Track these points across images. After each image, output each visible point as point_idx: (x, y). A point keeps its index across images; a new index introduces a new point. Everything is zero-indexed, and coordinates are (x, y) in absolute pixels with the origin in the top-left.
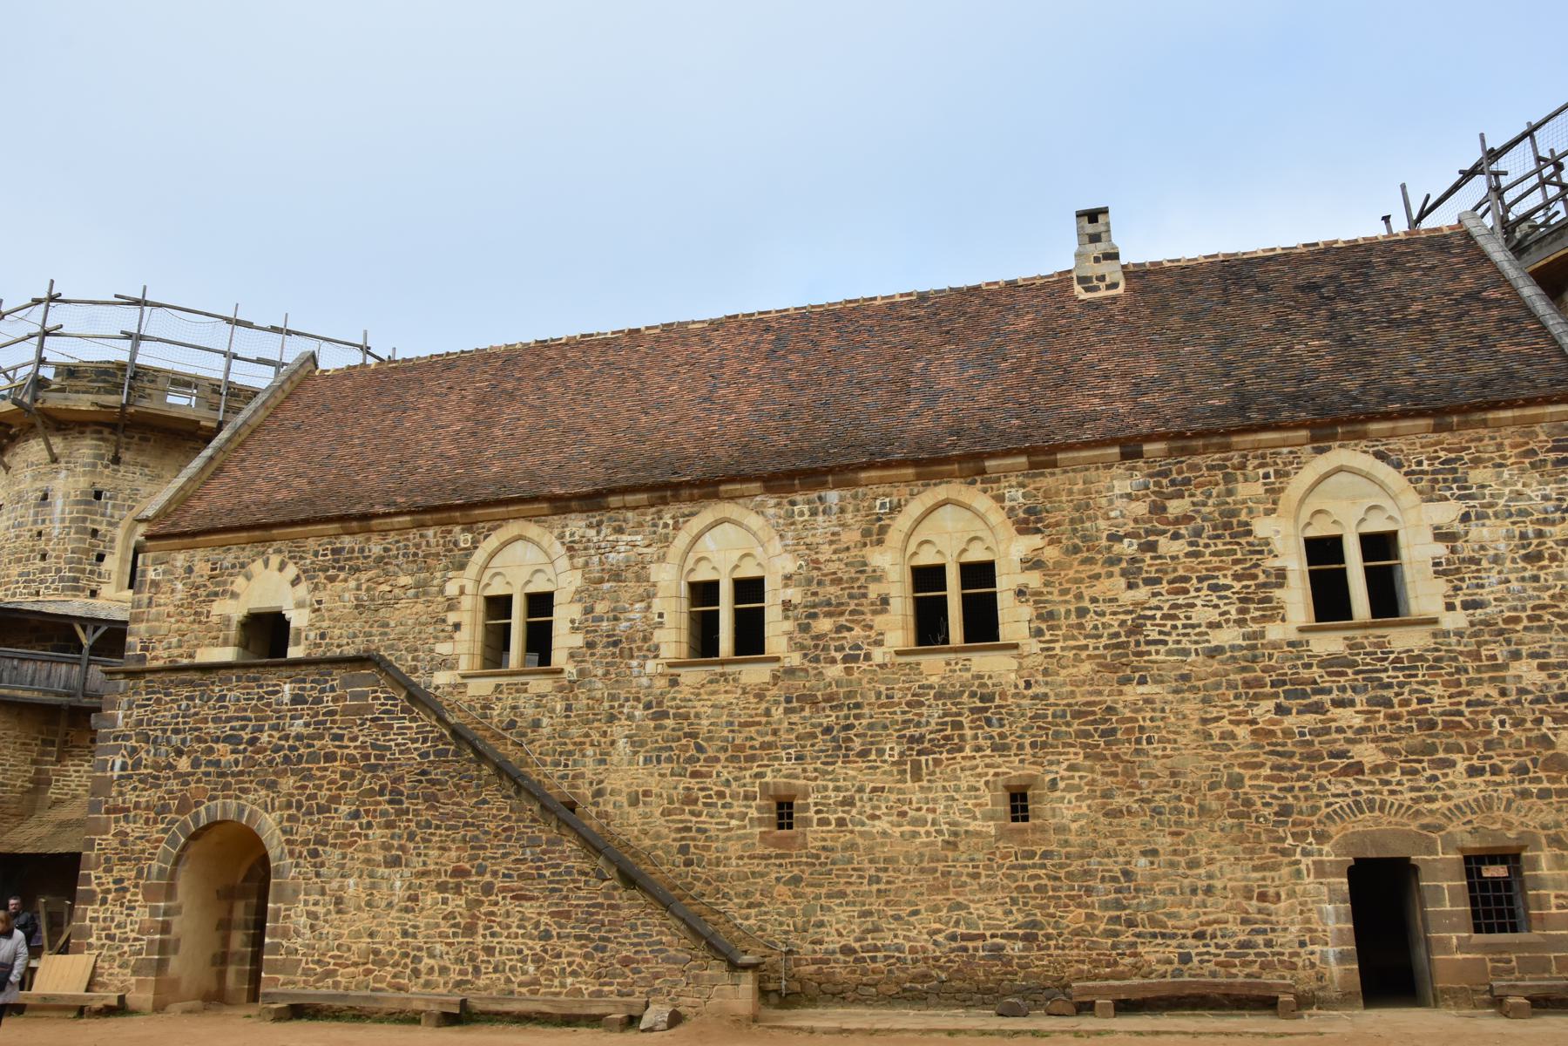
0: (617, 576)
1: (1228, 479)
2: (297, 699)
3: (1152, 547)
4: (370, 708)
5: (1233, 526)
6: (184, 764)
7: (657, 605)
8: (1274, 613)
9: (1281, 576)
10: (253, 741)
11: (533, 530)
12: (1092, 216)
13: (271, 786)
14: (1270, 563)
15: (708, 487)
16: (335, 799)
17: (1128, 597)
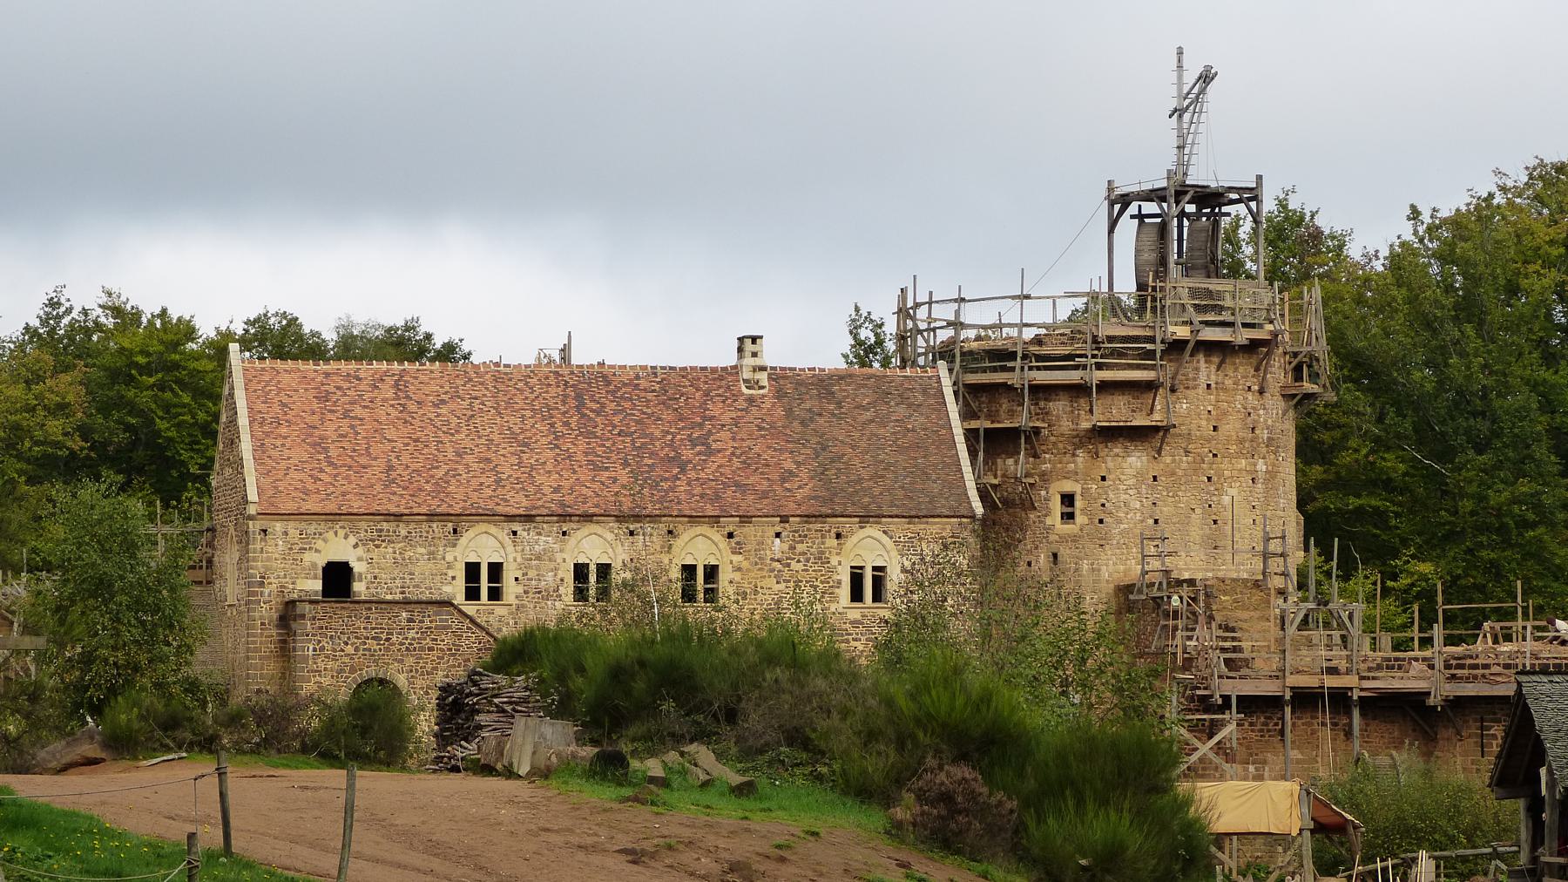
0: (538, 558)
1: (823, 537)
2: (410, 620)
3: (788, 565)
4: (450, 627)
5: (822, 559)
6: (350, 649)
7: (560, 574)
8: (835, 599)
9: (839, 582)
10: (388, 640)
11: (493, 529)
12: (754, 339)
13: (400, 661)
14: (835, 577)
15: (587, 518)
16: (436, 669)
17: (777, 587)
